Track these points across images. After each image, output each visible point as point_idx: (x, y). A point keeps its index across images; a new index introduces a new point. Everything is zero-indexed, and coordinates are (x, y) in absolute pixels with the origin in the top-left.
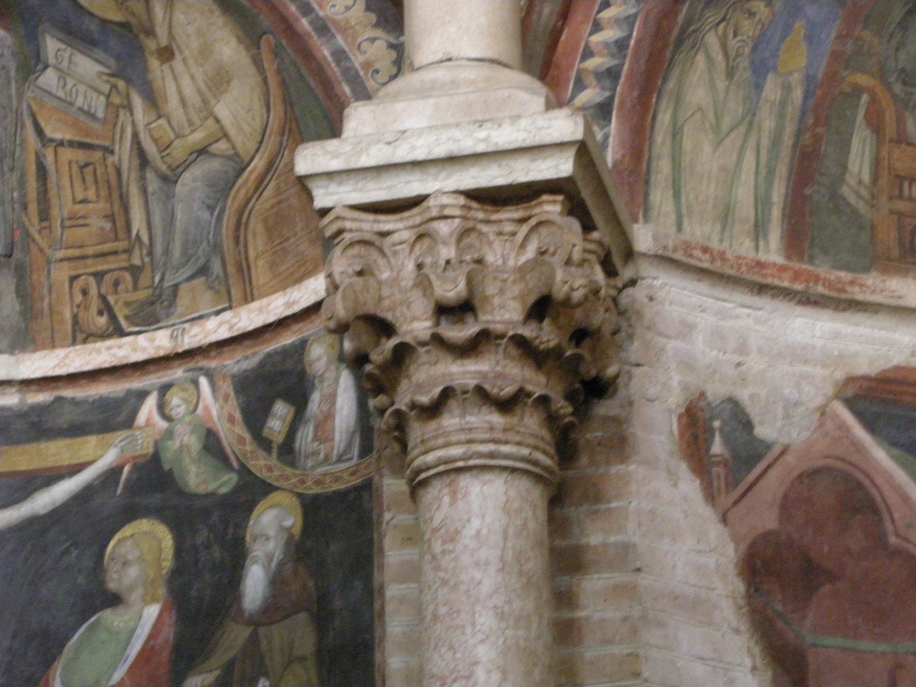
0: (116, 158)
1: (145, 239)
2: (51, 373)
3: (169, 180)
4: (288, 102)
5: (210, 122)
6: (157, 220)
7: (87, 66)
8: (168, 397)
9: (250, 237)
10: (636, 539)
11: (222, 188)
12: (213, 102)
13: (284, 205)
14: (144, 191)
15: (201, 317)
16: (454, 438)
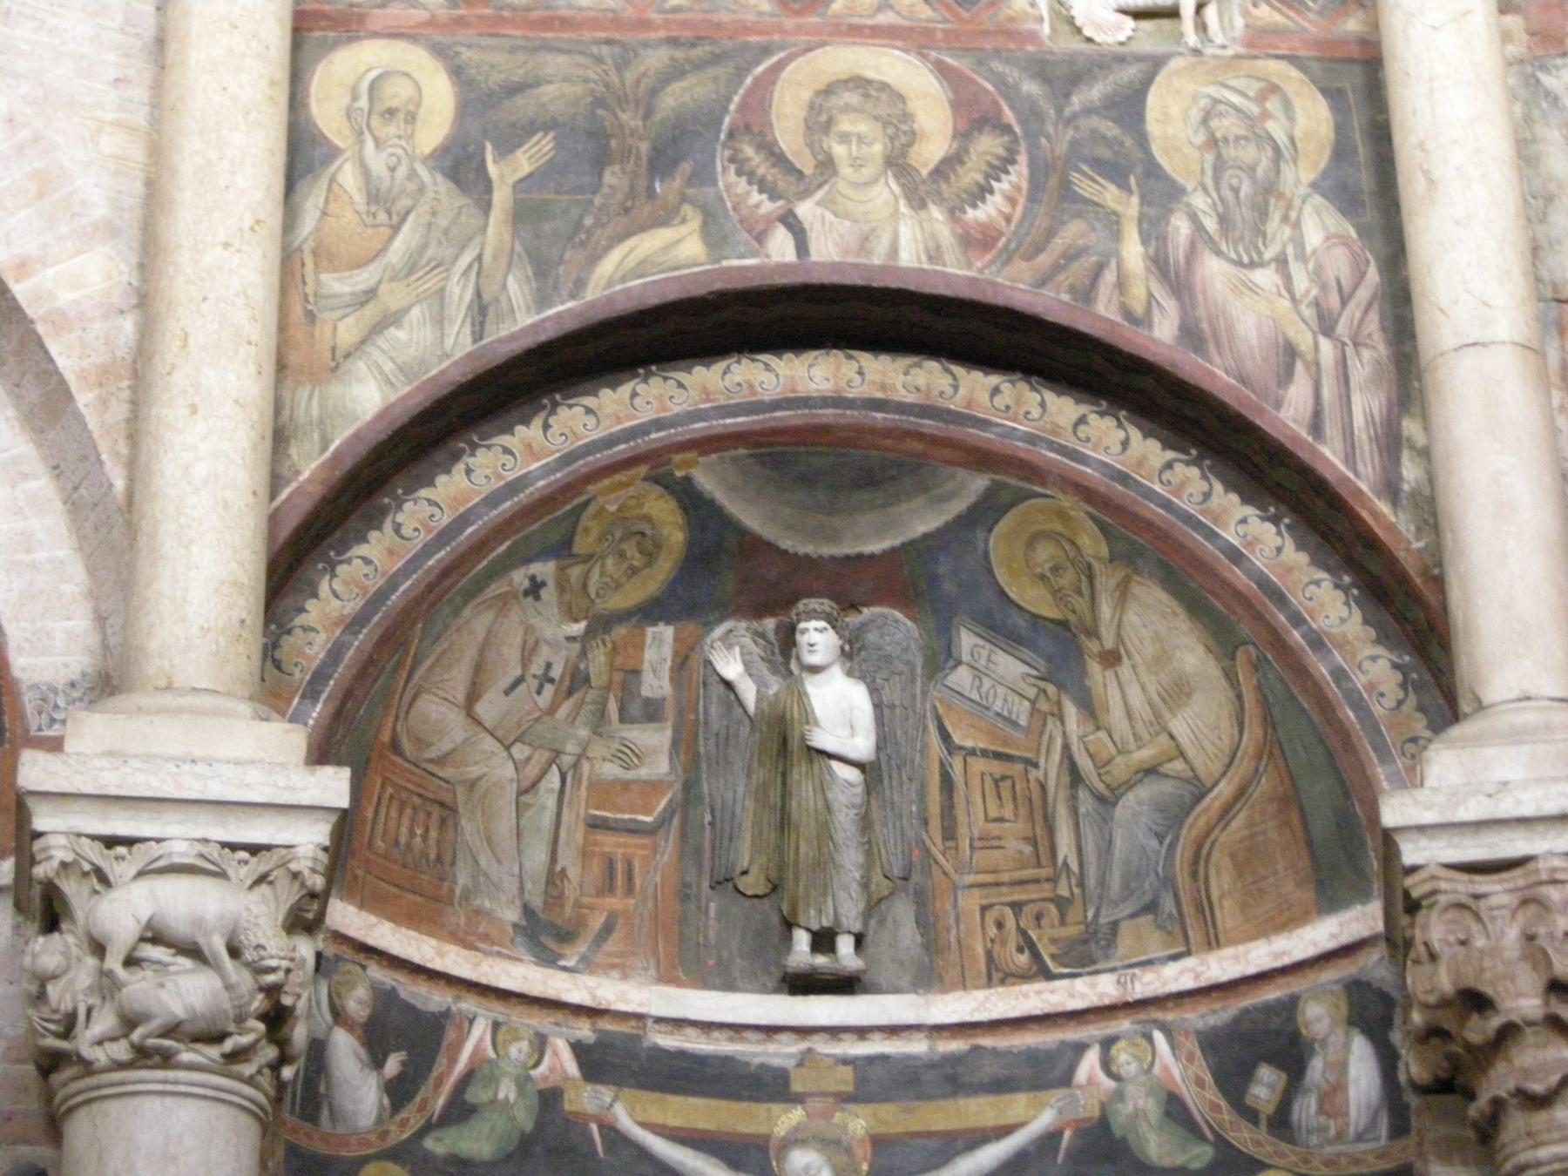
2: (968, 1018)
3: (1107, 802)
4: (1268, 722)
5: (1164, 738)
7: (1009, 666)
8: (1113, 1051)
9: (1212, 872)
11: (1173, 816)
12: (1167, 716)
13: (1260, 839)
14: (1074, 812)
15: (1149, 962)
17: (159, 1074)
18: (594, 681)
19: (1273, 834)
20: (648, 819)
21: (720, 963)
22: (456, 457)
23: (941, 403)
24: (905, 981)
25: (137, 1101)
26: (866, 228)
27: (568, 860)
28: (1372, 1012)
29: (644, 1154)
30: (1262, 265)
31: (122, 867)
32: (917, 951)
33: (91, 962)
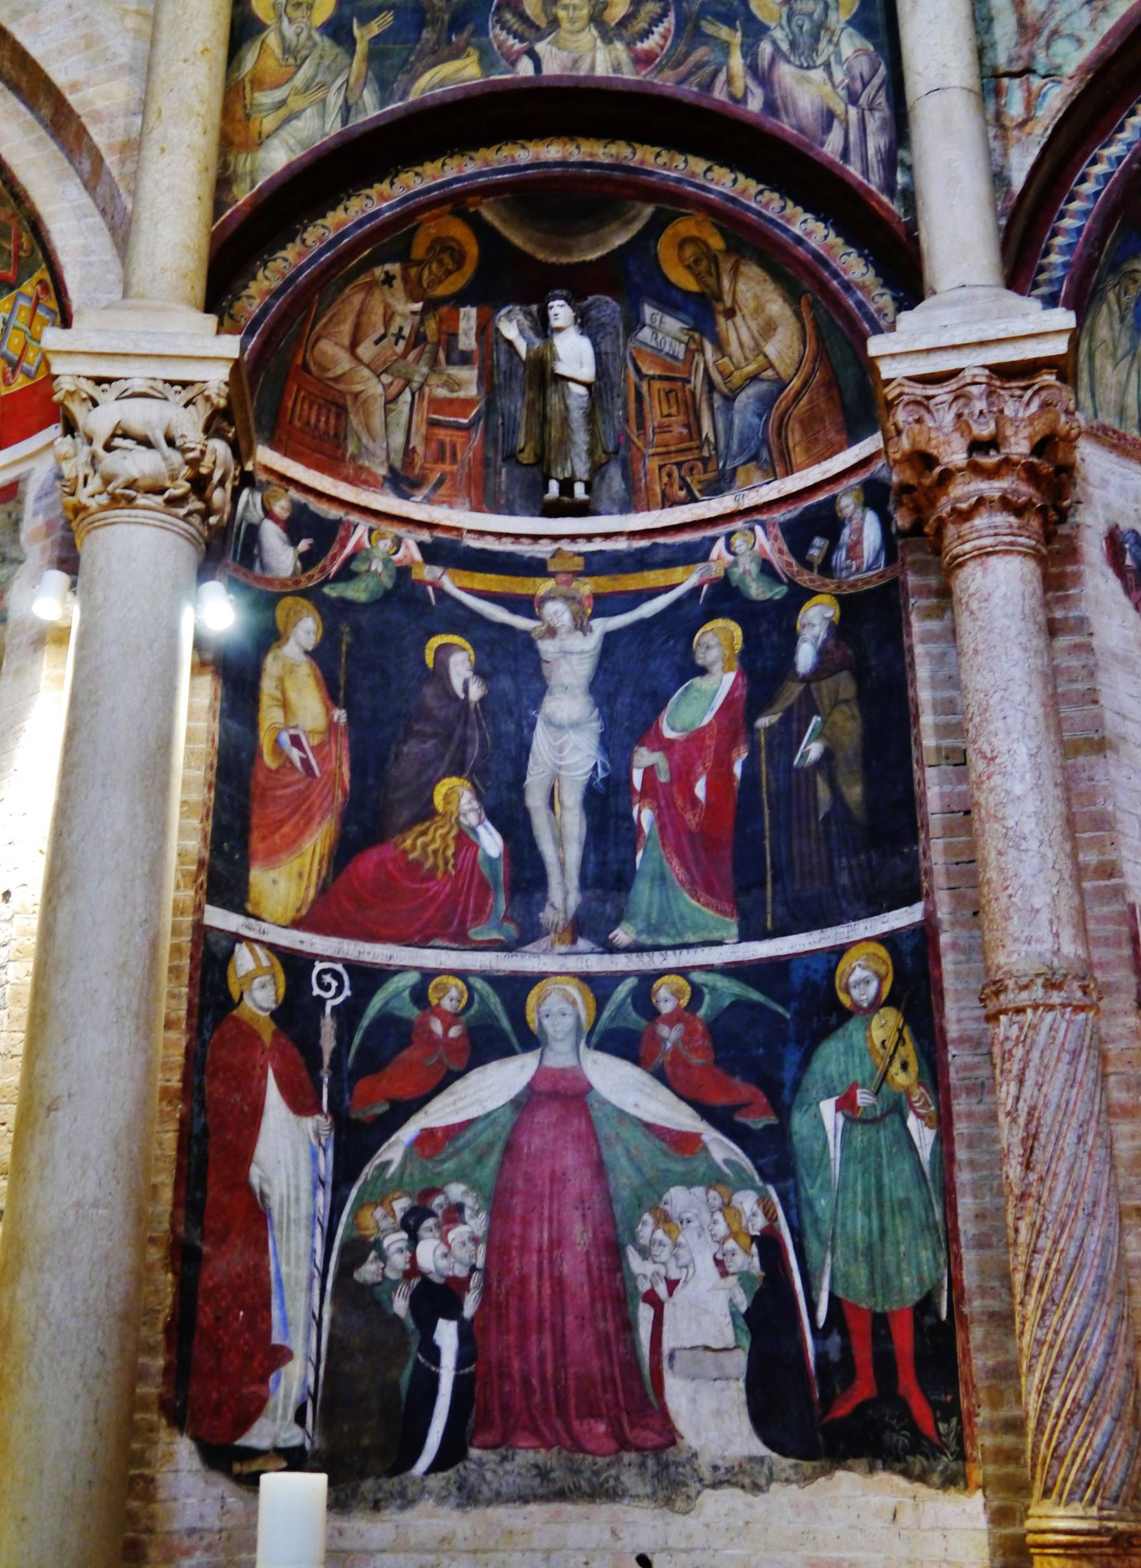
0: (691, 386)
1: (712, 439)
4: (820, 338)
5: (761, 358)
6: (721, 426)
7: (673, 324)
10: (1087, 614)
11: (766, 403)
16: (985, 533)
17: (126, 512)
18: (429, 339)
19: (823, 406)
20: (465, 421)
21: (508, 501)
22: (339, 202)
23: (624, 162)
24: (615, 509)
25: (114, 527)
26: (577, 55)
27: (416, 442)
28: (875, 495)
29: (460, 604)
30: (815, 67)
31: (107, 396)
32: (622, 493)
33: (87, 448)
